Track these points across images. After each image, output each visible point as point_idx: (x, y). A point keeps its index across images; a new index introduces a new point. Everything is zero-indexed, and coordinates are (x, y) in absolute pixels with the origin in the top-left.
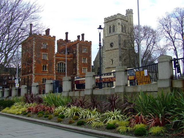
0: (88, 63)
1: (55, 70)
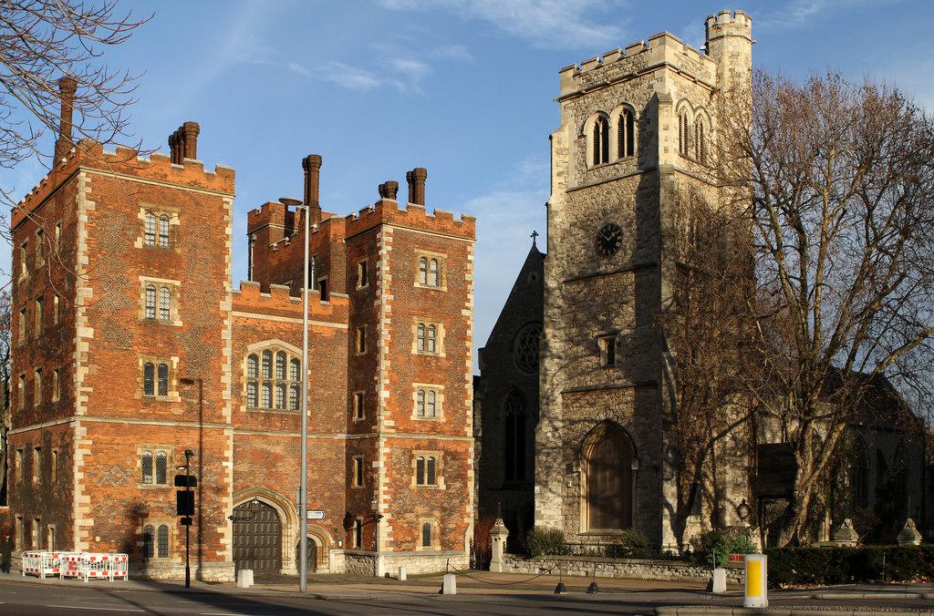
0: (447, 359)
1: (227, 394)
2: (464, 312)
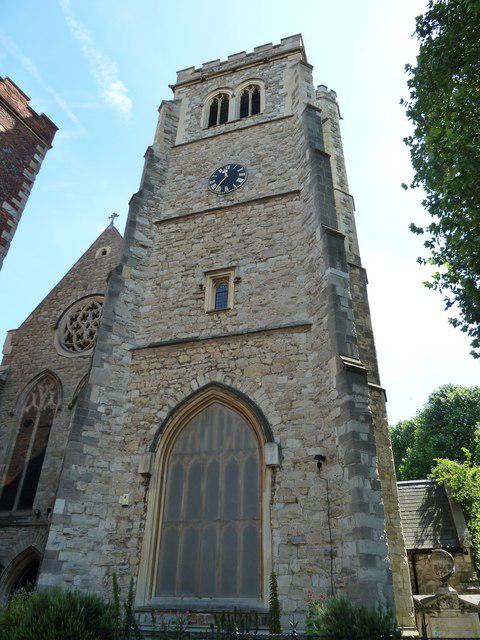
2: (6, 206)
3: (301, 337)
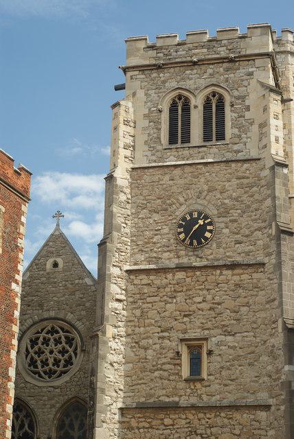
3: (262, 415)
